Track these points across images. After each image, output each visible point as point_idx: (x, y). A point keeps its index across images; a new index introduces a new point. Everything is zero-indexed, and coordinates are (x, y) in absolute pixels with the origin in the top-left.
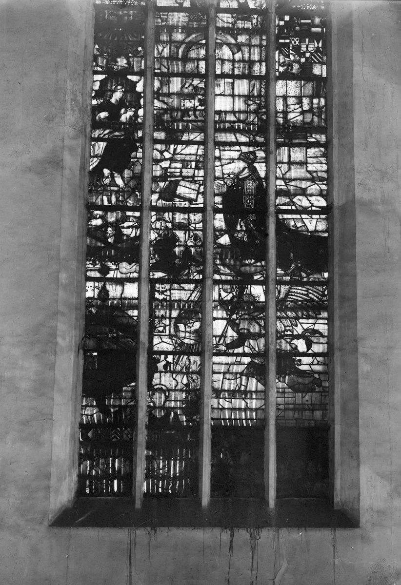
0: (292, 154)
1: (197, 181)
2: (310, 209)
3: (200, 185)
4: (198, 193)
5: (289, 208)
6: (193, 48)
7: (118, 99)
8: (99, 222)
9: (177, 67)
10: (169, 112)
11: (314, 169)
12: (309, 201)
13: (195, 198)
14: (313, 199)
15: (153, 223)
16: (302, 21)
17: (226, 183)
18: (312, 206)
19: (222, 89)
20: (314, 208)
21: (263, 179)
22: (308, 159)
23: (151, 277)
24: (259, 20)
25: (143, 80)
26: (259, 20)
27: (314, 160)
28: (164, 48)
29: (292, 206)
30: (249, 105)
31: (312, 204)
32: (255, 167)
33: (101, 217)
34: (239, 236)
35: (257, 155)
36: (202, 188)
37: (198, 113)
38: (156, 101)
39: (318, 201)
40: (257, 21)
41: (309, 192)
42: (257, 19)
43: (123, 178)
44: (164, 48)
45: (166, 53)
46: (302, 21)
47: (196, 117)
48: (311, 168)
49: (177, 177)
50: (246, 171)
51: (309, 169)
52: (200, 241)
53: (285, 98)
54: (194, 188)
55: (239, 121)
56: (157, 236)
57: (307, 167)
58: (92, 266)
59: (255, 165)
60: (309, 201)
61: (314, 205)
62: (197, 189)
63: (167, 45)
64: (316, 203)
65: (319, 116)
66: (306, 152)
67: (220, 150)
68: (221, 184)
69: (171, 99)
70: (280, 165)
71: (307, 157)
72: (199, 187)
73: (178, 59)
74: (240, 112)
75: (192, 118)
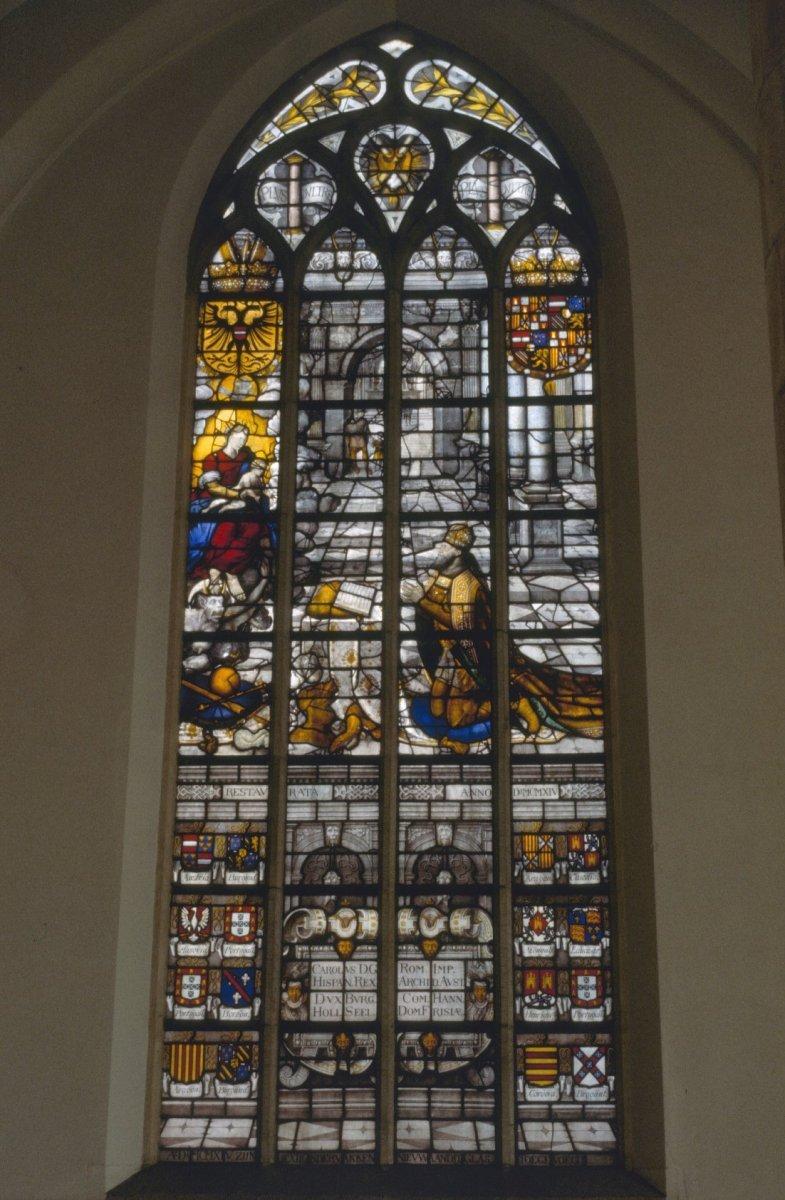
0: (536, 530)
1: (372, 582)
2: (569, 627)
3: (376, 591)
4: (374, 604)
5: (532, 625)
6: (367, 357)
7: (237, 449)
8: (200, 661)
9: (336, 392)
10: (323, 464)
11: (575, 555)
12: (568, 612)
13: (367, 612)
14: (574, 609)
15: (295, 659)
16: (552, 304)
17: (422, 585)
18: (573, 621)
19: (414, 422)
20: (577, 626)
21: (488, 575)
22: (566, 538)
23: (290, 753)
24: (475, 307)
25: (278, 413)
26: (475, 307)
27: (574, 540)
28: (315, 361)
29: (536, 621)
30: (459, 448)
31: (571, 617)
32: (472, 557)
33: (205, 652)
34: (444, 676)
35: (477, 533)
36: (380, 594)
37: (372, 465)
38: (301, 448)
39: (583, 611)
40: (471, 308)
41: (564, 596)
42: (471, 305)
43: (242, 582)
44: (315, 361)
45: (320, 365)
46: (552, 304)
47: (368, 470)
48: (570, 552)
49: (334, 575)
50: (457, 561)
51: (566, 555)
52: (377, 687)
53: (525, 432)
54: (367, 595)
55: (445, 475)
56: (302, 680)
57: (563, 552)
58: (189, 738)
59: (474, 551)
60: (568, 612)
61: (576, 618)
62: (371, 596)
63: (321, 356)
64: (579, 616)
65: (585, 463)
66: (562, 526)
67: (411, 528)
68: (412, 585)
69: (326, 443)
70: (516, 550)
71: (563, 535)
72: (375, 594)
73: (337, 377)
74: (446, 458)
75: (363, 474)
